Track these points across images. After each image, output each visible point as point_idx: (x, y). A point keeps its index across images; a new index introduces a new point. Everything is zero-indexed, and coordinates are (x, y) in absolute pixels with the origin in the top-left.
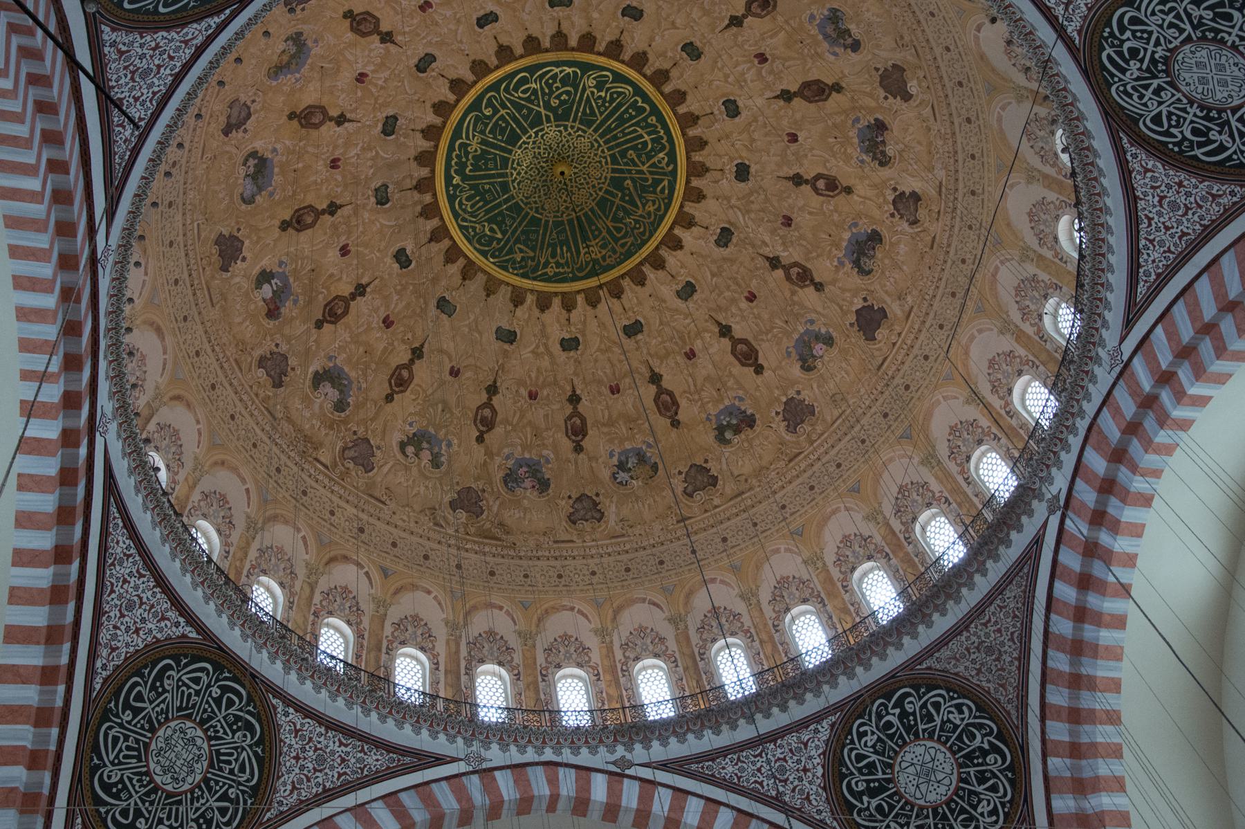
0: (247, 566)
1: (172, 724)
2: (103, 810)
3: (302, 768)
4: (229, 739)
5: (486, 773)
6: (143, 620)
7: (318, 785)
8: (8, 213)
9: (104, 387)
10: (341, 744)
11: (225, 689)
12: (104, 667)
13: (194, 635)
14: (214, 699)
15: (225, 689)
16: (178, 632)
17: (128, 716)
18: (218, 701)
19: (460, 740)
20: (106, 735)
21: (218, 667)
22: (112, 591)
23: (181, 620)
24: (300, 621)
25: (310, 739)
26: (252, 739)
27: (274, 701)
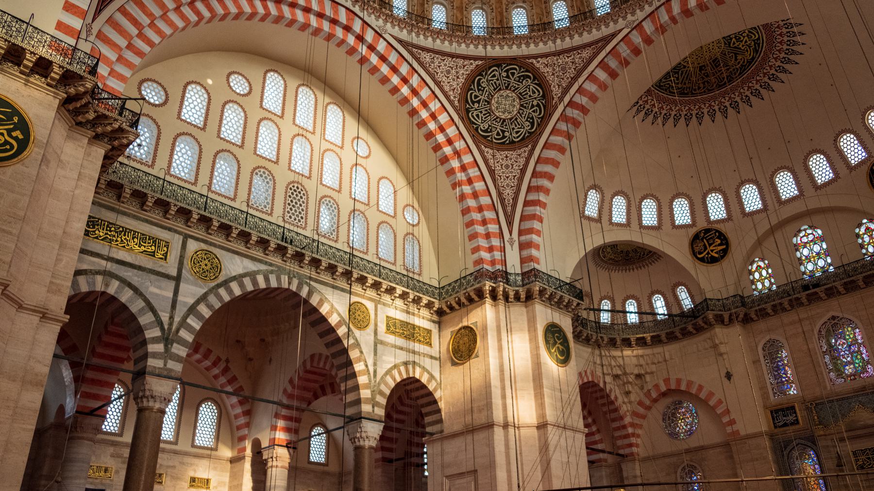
0: (504, 7)
1: (496, 96)
2: (489, 138)
3: (558, 77)
4: (521, 86)
5: (639, 26)
6: (457, 73)
7: (568, 78)
8: (272, 20)
9: (371, 20)
10: (568, 57)
11: (507, 71)
12: (455, 97)
13: (480, 62)
14: (505, 77)
15: (507, 71)
16: (474, 66)
17: (476, 105)
18: (508, 77)
19: (620, 20)
20: (473, 116)
21: (499, 66)
22: (437, 73)
23: (472, 61)
24: (539, 12)
25: (554, 64)
26: (530, 78)
27: (530, 61)
